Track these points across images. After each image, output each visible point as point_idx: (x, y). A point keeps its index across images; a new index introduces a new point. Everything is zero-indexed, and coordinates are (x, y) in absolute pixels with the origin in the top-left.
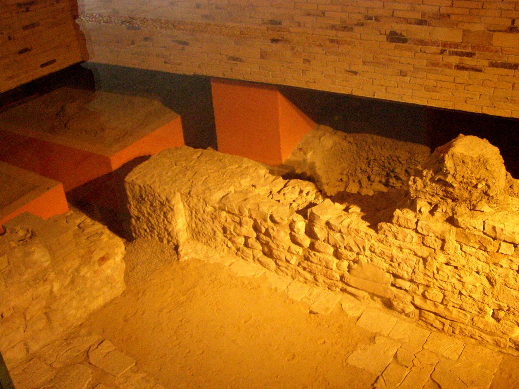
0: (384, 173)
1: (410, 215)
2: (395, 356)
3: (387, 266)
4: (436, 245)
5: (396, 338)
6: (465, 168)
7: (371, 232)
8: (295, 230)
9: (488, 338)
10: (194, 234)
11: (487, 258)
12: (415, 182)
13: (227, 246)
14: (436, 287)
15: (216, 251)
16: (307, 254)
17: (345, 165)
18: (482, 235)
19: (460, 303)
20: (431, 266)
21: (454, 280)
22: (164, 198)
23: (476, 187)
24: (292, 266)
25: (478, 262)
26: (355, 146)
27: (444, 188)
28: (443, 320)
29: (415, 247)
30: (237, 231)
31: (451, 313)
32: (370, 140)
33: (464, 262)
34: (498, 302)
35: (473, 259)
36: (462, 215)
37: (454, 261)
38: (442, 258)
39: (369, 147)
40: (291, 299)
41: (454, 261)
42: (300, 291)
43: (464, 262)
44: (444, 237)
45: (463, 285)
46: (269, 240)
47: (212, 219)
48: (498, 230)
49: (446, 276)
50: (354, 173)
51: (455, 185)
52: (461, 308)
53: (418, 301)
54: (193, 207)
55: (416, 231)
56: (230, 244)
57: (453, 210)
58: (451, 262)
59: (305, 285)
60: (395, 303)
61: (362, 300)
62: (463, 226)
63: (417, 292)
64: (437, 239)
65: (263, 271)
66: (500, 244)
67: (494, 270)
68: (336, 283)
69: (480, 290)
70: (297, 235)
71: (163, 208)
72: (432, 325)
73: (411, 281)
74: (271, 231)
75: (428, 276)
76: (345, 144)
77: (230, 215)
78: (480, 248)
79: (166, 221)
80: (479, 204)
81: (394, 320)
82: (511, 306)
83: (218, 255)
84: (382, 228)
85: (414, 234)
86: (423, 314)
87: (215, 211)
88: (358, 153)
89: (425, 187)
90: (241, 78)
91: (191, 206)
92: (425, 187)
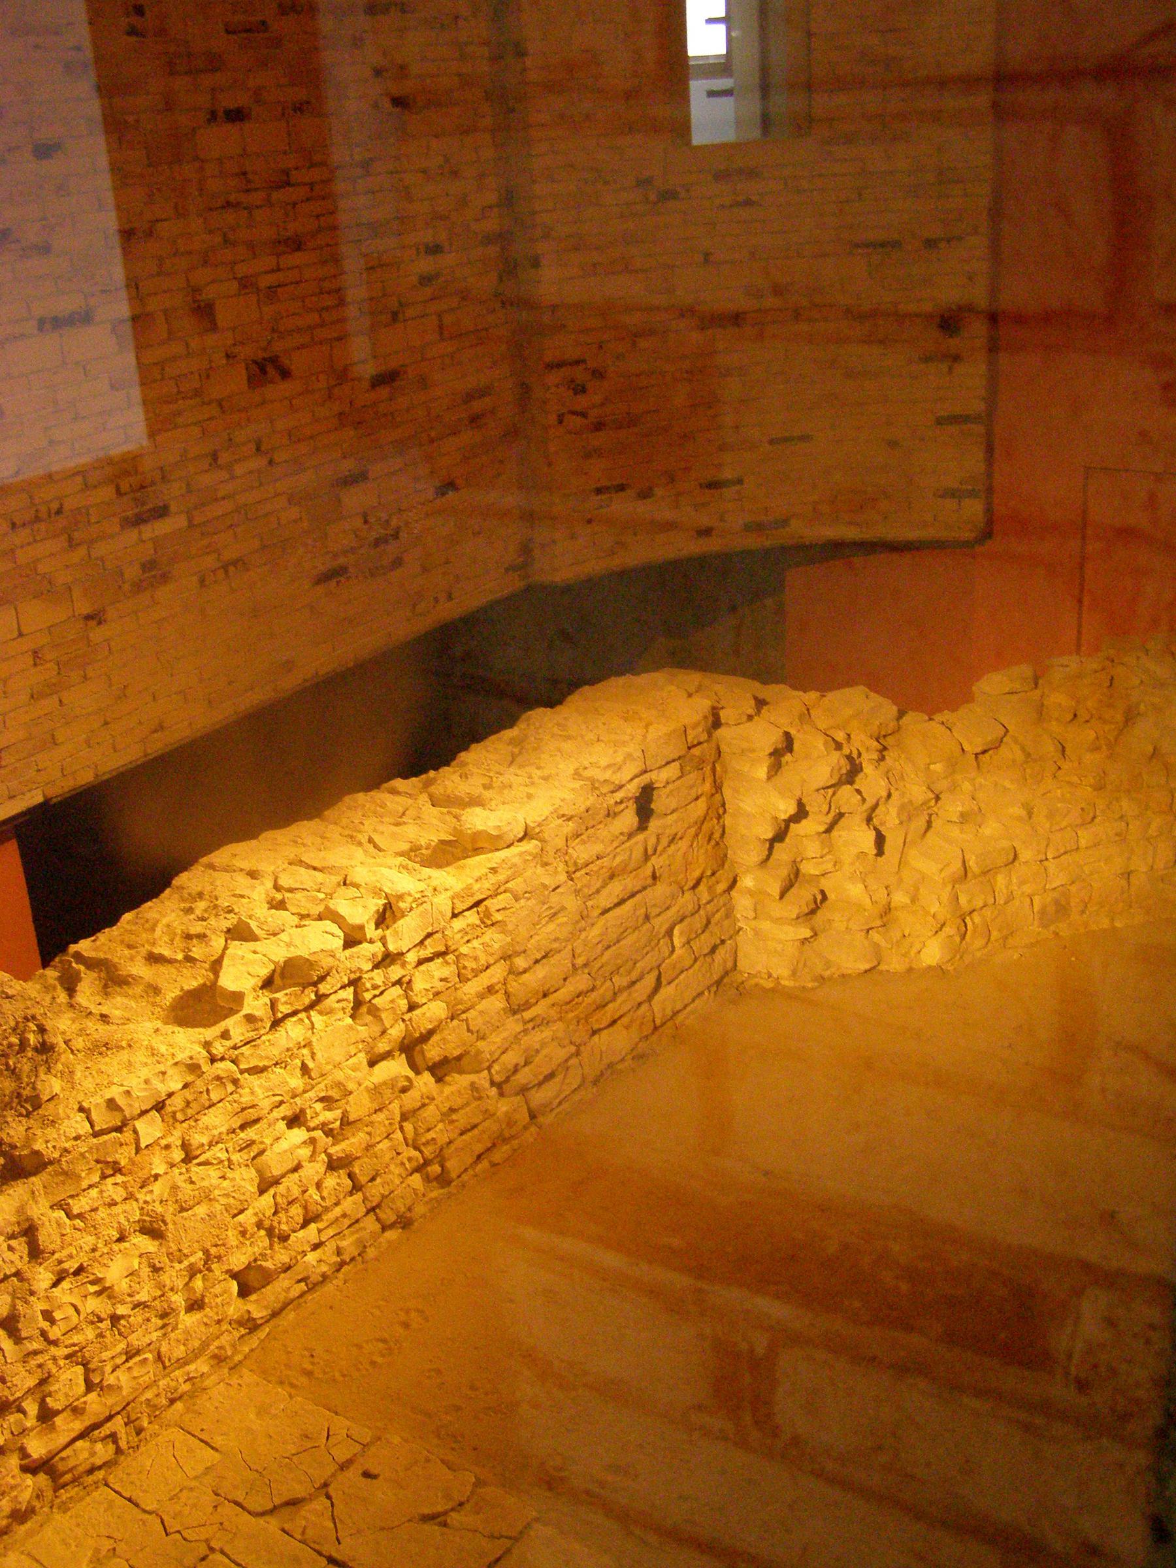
4: (15, 1257)
9: (201, 1366)
11: (125, 1185)
14: (62, 1363)
18: (95, 1140)
19: (122, 1346)
20: (33, 1318)
21: (93, 1305)
23: (23, 1044)
25: (115, 1210)
28: (106, 1430)
31: (120, 1388)
33: (88, 1240)
34: (186, 1263)
35: (103, 1213)
37: (71, 1256)
38: (42, 1277)
41: (71, 1256)
43: (88, 1240)
44: (27, 1220)
45: (109, 1297)
48: (121, 1101)
49: (72, 1311)
53: (37, 1448)
58: (65, 1266)
62: (56, 1155)
63: (28, 1424)
64: (13, 1243)
66: (135, 1132)
67: (148, 1198)
69: (146, 1271)
75: (36, 1353)
78: (104, 1177)
80: (39, 1085)
82: (208, 1245)
86: (61, 1467)
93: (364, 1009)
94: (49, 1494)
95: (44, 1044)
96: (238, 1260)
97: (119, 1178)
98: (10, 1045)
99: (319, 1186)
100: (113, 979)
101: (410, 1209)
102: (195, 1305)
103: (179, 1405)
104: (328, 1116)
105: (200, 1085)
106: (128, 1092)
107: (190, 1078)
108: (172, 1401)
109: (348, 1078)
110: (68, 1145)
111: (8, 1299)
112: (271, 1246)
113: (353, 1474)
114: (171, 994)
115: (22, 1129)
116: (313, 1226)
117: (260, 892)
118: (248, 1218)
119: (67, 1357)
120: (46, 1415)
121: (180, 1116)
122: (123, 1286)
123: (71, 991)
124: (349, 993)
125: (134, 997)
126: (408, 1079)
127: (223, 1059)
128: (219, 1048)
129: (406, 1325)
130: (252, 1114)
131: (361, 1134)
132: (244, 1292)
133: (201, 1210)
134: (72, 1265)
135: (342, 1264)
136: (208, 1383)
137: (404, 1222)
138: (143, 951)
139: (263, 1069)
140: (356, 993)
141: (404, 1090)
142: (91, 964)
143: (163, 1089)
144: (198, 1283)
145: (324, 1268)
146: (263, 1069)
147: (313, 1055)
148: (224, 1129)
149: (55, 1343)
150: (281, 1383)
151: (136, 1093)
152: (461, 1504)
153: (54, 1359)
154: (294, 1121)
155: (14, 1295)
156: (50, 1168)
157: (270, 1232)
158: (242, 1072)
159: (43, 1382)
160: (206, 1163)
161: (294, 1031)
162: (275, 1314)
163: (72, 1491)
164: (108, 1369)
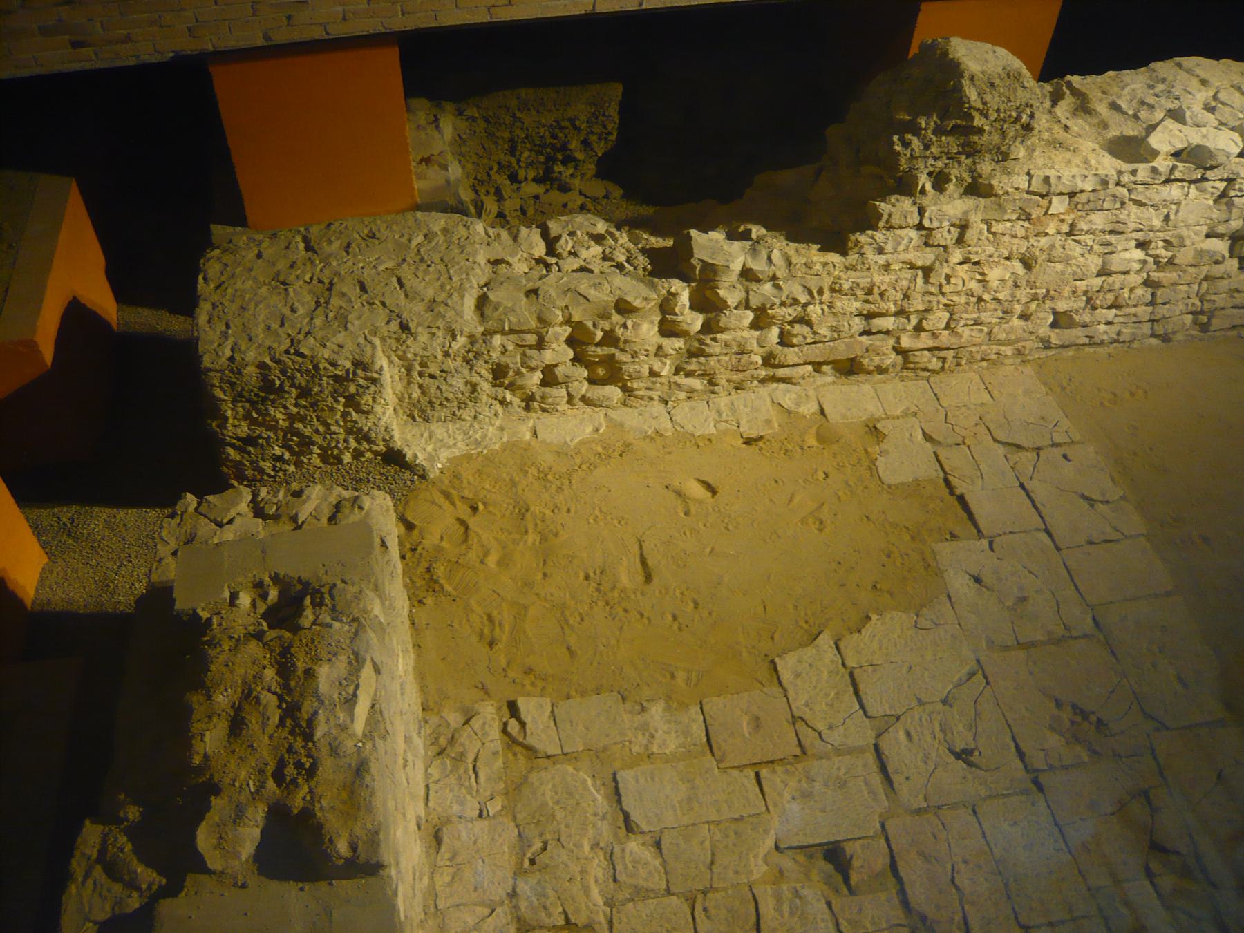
0: (542, 158)
1: (906, 203)
2: (927, 437)
3: (857, 304)
4: (948, 237)
5: (898, 412)
6: (997, 95)
7: (834, 257)
8: (677, 310)
9: (1008, 351)
10: (416, 413)
11: (1027, 230)
12: (906, 144)
13: (503, 402)
15: (480, 423)
16: (696, 344)
17: (469, 166)
19: (975, 316)
20: (940, 275)
21: (973, 285)
22: (348, 365)
23: (1018, 119)
24: (663, 380)
25: (1015, 241)
26: (483, 124)
27: (963, 139)
28: (943, 354)
29: (910, 257)
30: (533, 363)
32: (514, 103)
33: (990, 249)
35: (1007, 238)
36: (991, 176)
39: (514, 116)
40: (702, 436)
42: (698, 417)
44: (967, 221)
46: (613, 350)
47: (468, 362)
48: (1053, 181)
50: (485, 178)
51: (987, 128)
52: (977, 322)
53: (906, 342)
54: (415, 355)
55: (920, 227)
56: (509, 396)
57: (972, 171)
59: (693, 403)
60: (865, 361)
61: (802, 382)
65: (602, 415)
66: (1050, 202)
68: (755, 373)
69: (1010, 283)
70: (680, 318)
71: (346, 389)
72: (925, 369)
73: (901, 313)
74: (619, 331)
75: (931, 294)
76: (463, 125)
77: (512, 337)
78: (1018, 219)
79: (354, 413)
80: (1013, 148)
81: (867, 388)
83: (496, 427)
84: (857, 242)
85: (913, 234)
86: (912, 358)
87: (472, 343)
88: (490, 135)
89: (927, 147)
90: (317, 34)
91: (410, 356)
92: (927, 147)
93: (1225, 200)
94: (898, 368)
95: (1028, 125)
96: (1062, 306)
97: (1026, 224)
98: (1010, 116)
99: (1132, 290)
100: (1083, 107)
101: (1174, 333)
102: (1025, 317)
103: (985, 364)
104: (1163, 252)
105: (1102, 195)
106: (1059, 177)
107: (1098, 188)
108: (983, 360)
109: (1189, 237)
110: (1010, 190)
111: (933, 257)
112: (1084, 309)
113: (1057, 452)
114: (1113, 133)
115: (990, 168)
116: (1114, 311)
117: (1203, 95)
118: (1082, 285)
119: (945, 305)
120: (919, 329)
121: (1080, 207)
122: (994, 284)
123: (1054, 103)
124: (1221, 186)
125: (1090, 124)
126: (1224, 257)
127: (1123, 186)
128: (1126, 179)
129: (1132, 394)
130: (1120, 227)
131: (1175, 274)
132: (1054, 325)
133: (1059, 267)
134: (975, 258)
135: (1116, 341)
136: (1006, 361)
137: (1166, 338)
138: (1110, 99)
139: (1144, 205)
140: (1226, 188)
141: (1216, 262)
142: (1075, 92)
143: (1080, 185)
144: (1033, 306)
145: (1105, 337)
146: (1144, 205)
147: (1177, 211)
148: (1100, 227)
149: (943, 294)
150: (1045, 384)
151: (1063, 180)
152: (1108, 502)
153: (938, 302)
154: (1141, 245)
155: (937, 258)
156: (993, 198)
157: (1089, 300)
158: (1130, 200)
159: (926, 311)
160: (1078, 242)
161: (1175, 191)
162: (1063, 347)
163: (910, 374)
164: (962, 323)
